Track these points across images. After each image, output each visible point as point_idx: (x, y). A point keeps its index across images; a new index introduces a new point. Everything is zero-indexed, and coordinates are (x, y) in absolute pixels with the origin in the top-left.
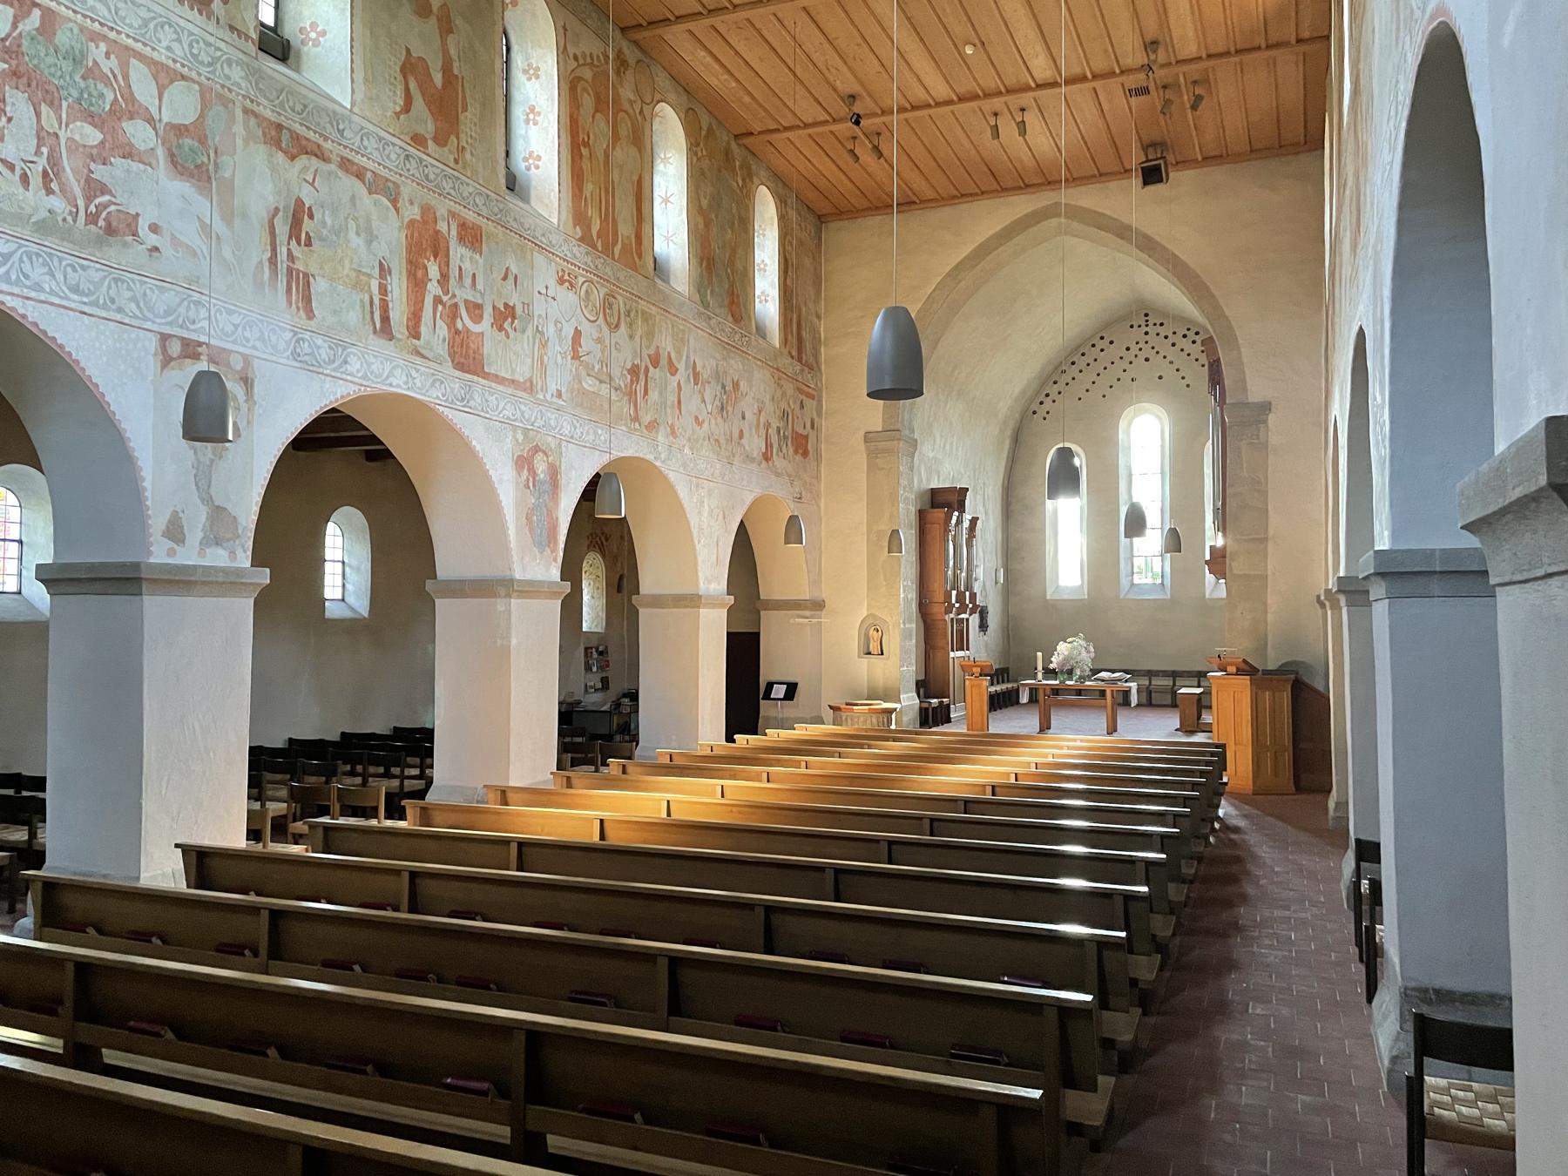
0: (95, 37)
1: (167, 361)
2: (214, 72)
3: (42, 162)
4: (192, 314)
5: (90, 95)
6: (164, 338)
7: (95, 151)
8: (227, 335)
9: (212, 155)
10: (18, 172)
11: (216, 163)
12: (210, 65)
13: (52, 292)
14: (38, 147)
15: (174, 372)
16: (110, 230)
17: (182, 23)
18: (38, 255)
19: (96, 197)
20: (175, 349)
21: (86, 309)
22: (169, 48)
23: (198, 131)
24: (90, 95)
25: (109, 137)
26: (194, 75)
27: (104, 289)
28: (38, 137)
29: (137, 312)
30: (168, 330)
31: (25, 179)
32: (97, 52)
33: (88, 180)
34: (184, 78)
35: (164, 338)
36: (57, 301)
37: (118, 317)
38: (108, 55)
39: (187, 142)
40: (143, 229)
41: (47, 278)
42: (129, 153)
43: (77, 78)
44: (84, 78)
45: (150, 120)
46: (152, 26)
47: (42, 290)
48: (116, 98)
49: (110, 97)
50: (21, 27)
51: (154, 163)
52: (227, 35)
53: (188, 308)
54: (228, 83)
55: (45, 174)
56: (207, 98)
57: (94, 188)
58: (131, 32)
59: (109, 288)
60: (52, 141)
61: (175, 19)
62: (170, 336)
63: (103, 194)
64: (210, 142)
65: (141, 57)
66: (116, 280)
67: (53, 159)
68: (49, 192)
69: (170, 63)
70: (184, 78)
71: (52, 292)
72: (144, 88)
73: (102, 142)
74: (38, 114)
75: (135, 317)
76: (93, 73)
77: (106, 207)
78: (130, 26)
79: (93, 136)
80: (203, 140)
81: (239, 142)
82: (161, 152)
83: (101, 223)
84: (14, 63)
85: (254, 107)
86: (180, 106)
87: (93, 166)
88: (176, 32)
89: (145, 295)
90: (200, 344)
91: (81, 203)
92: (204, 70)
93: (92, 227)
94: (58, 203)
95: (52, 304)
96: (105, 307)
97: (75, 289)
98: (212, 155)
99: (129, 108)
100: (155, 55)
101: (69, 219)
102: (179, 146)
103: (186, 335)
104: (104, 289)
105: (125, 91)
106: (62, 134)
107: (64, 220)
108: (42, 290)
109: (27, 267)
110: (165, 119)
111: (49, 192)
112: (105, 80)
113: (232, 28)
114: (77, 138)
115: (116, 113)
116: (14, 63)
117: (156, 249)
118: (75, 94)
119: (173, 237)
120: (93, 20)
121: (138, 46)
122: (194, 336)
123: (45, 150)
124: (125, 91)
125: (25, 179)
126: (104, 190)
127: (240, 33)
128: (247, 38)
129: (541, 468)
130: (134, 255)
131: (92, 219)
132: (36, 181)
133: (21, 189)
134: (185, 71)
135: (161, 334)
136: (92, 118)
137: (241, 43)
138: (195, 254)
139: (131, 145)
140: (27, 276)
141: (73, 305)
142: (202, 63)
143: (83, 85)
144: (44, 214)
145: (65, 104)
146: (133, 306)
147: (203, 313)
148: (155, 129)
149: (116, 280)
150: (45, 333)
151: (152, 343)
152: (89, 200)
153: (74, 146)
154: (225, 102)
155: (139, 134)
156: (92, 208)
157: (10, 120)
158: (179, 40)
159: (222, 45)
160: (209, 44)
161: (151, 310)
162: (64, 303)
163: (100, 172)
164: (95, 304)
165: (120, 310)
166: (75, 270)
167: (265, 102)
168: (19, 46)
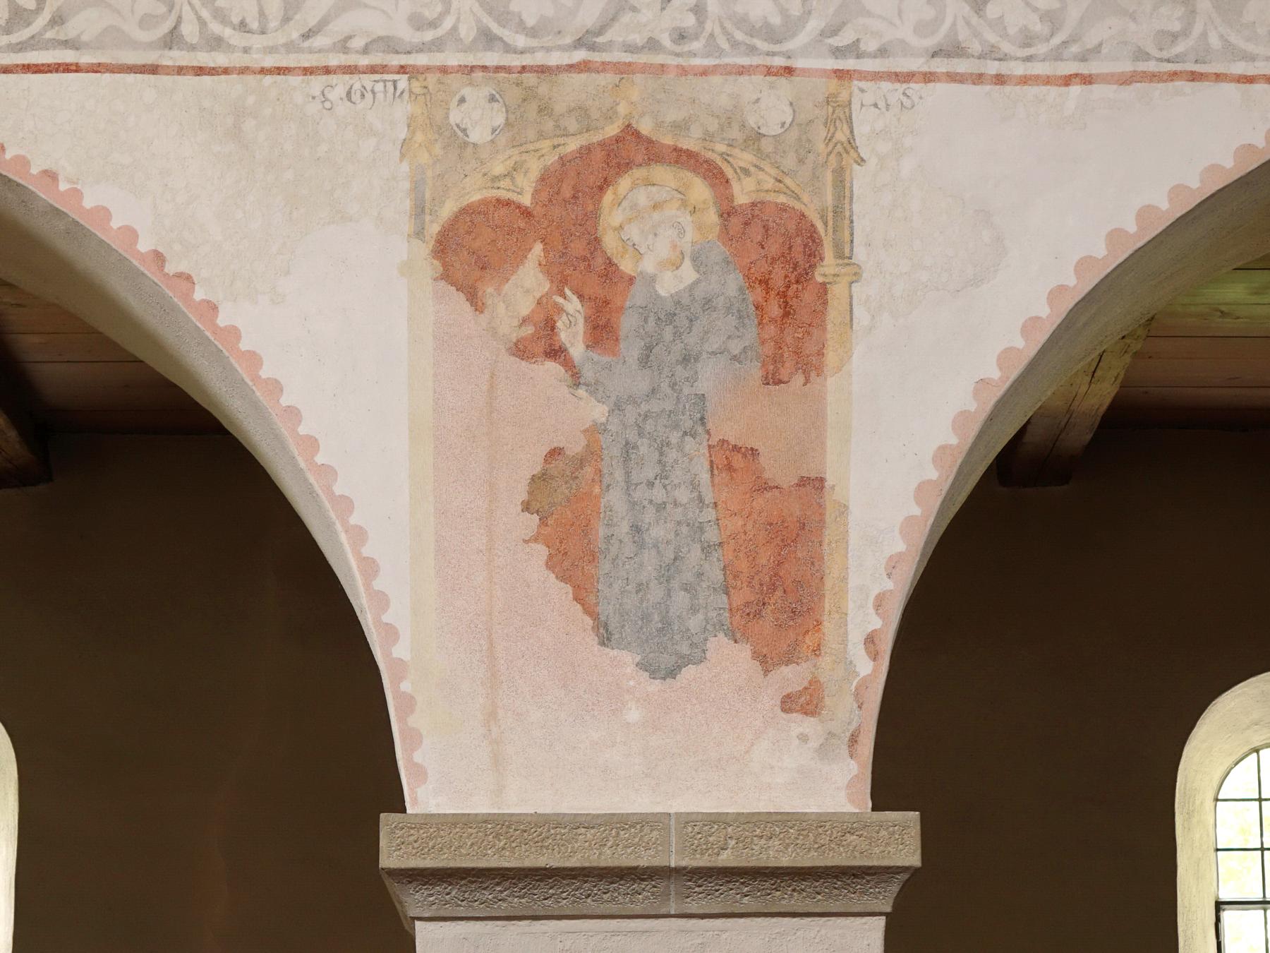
129: (660, 237)
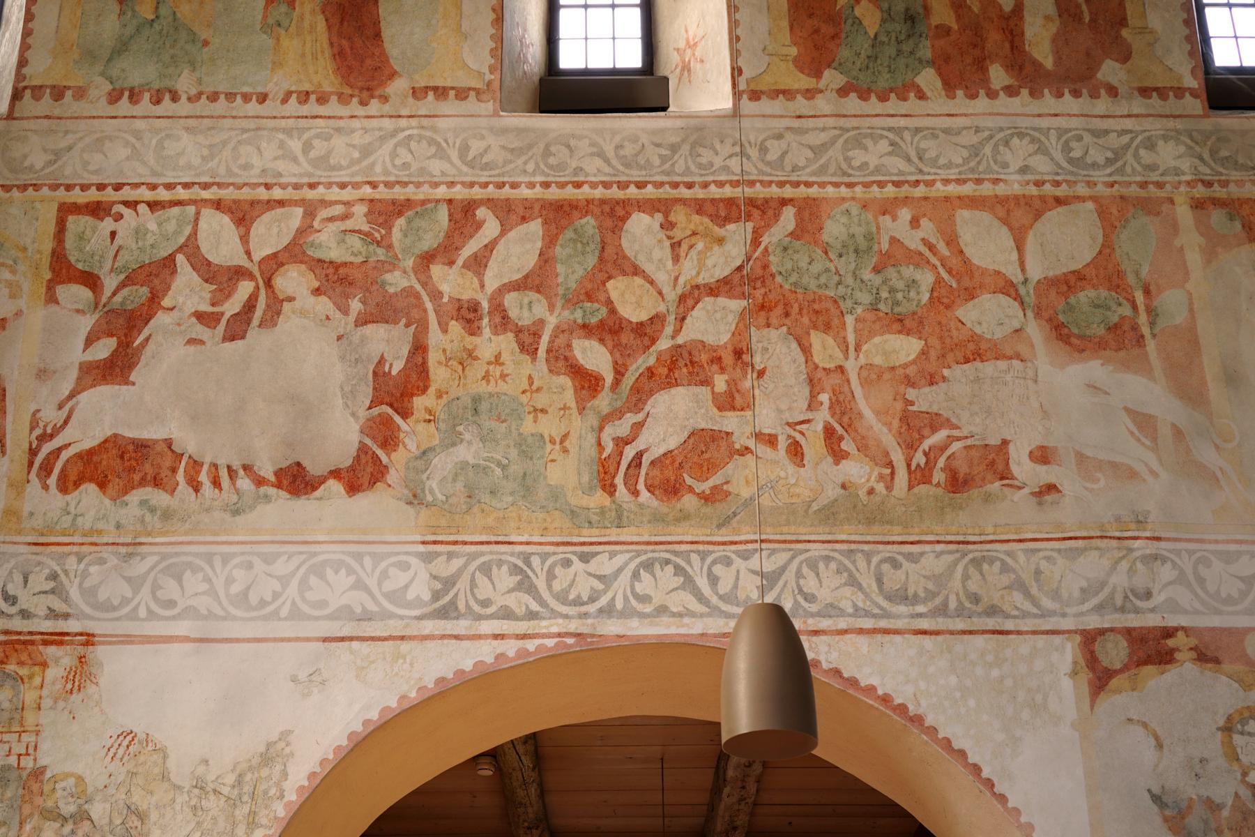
0: (888, 208)
1: (1100, 679)
2: (1121, 171)
3: (823, 416)
4: (1140, 582)
5: (892, 291)
6: (1089, 639)
7: (911, 371)
8: (1229, 600)
9: (1140, 297)
10: (782, 443)
11: (1150, 310)
12: (1110, 162)
13: (858, 612)
14: (813, 396)
15: (1119, 699)
16: (957, 483)
17: (1044, 123)
18: (828, 559)
19: (922, 438)
20: (1114, 653)
21: (925, 624)
22: (1024, 170)
23: (1106, 271)
24: (892, 291)
25: (934, 341)
26: (1081, 190)
27: (956, 583)
28: (811, 381)
29: (1027, 606)
30: (1094, 622)
31: (796, 451)
32: (898, 226)
33: (907, 418)
34: (1059, 201)
35: (1089, 639)
36: (868, 623)
37: (991, 623)
38: (915, 223)
39: (1084, 297)
40: (1022, 467)
41: (848, 591)
42: (975, 350)
43: (867, 275)
44: (877, 270)
45: (1008, 288)
46: (988, 150)
47: (842, 613)
48: (939, 281)
49: (926, 279)
50: (765, 240)
51: (1023, 349)
52: (1138, 105)
53: (1131, 571)
54: (1154, 177)
55: (829, 432)
56: (1113, 214)
57: (913, 426)
58: (953, 174)
59: (966, 577)
60: (835, 379)
61: (1024, 123)
62: (1102, 632)
63: (934, 429)
64: (1131, 279)
65: (973, 202)
66: (977, 563)
67: (843, 408)
68: (839, 456)
69: (1033, 190)
70: (1059, 201)
71: (858, 612)
72: (986, 244)
73: (924, 353)
74: (806, 350)
75: (1025, 615)
76: (895, 256)
77: (943, 448)
78: (950, 165)
79: (905, 348)
80: (1115, 281)
81: (1194, 258)
82: (1035, 331)
83: (938, 476)
84: (759, 294)
85: (1219, 192)
86: (1067, 241)
87: (911, 394)
88: (1033, 140)
89: (1038, 572)
90: (1169, 633)
91: (898, 457)
92: (1100, 176)
93: (922, 489)
94: (857, 470)
95: (861, 631)
96: (960, 612)
97: (902, 596)
98: (1140, 297)
99: (966, 282)
100: (1001, 189)
101: (880, 488)
102: (1070, 308)
103: (1133, 621)
104: (956, 583)
105: (955, 262)
106: (851, 366)
107: (871, 492)
108: (842, 613)
109: (810, 584)
110: (1036, 271)
111: (839, 456)
112: (916, 259)
113: (1145, 92)
114: (878, 360)
115: (942, 299)
116: (759, 294)
117: (1052, 488)
118: (866, 298)
119: (1081, 458)
120: (881, 184)
121: (968, 189)
122: (1153, 621)
123: (824, 398)
124: (955, 262)
125: (796, 451)
126: (935, 422)
127: (1162, 93)
128: (1180, 92)
130: (1009, 510)
131: (920, 476)
132: (814, 445)
133: (791, 468)
134: (1062, 191)
135: (1084, 633)
136: (901, 323)
137: (1172, 105)
138: (1133, 475)
139: (974, 338)
140: (810, 598)
141: (899, 624)
142: (1094, 165)
143: (877, 280)
144: (832, 492)
145: (849, 320)
146: (1018, 597)
147: (1166, 573)
148: (1018, 298)
149: (977, 563)
150: (853, 682)
151: (1067, 654)
152: (910, 447)
153: (872, 376)
154: (1147, 206)
155: (987, 315)
156: (919, 459)
157: (761, 374)
158: (1042, 150)
159: (1129, 124)
160: (1099, 134)
161: (1055, 595)
162: (883, 624)
163: (925, 399)
164: (942, 610)
165: (992, 611)
166: (896, 565)
167: (1235, 175)
168: (765, 267)
